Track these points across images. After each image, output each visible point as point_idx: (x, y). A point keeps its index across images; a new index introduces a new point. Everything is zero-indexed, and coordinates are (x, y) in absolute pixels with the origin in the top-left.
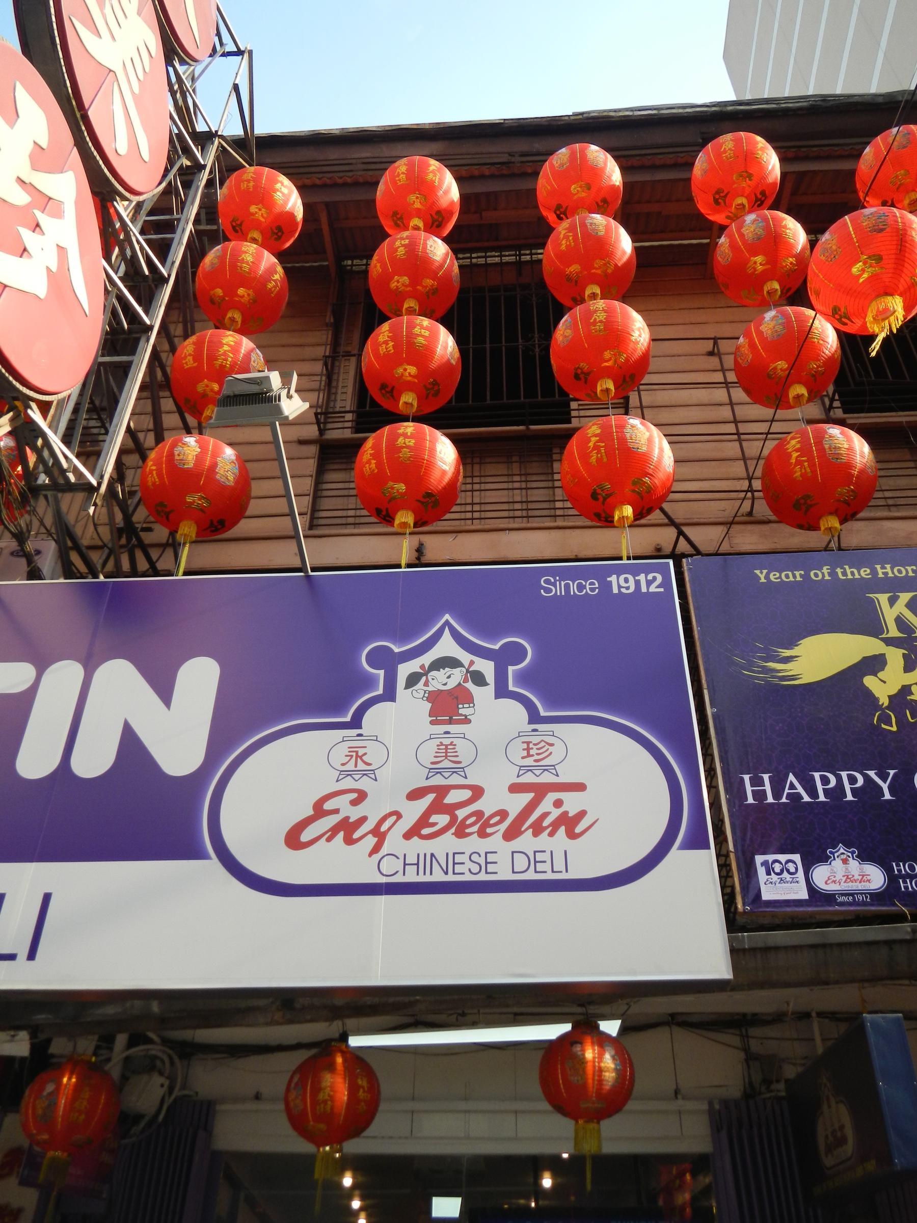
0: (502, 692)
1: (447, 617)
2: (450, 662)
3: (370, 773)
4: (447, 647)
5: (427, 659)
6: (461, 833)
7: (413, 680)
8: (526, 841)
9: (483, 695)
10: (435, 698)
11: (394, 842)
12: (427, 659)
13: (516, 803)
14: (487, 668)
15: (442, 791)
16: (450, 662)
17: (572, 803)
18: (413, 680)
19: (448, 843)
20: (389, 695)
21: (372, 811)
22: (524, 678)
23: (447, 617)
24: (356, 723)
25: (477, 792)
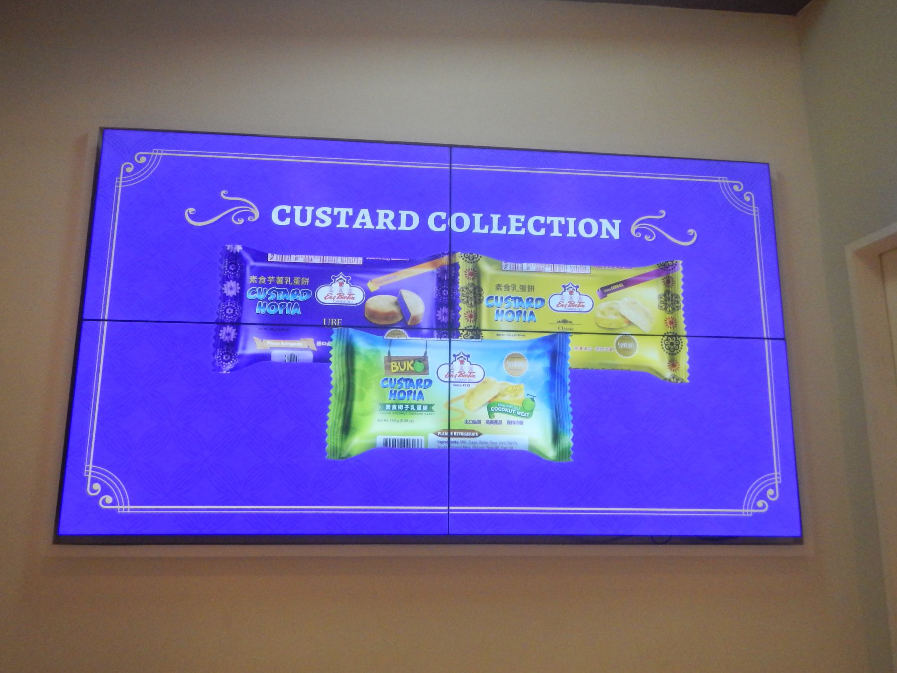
0: (347, 283)
1: (341, 273)
2: (341, 279)
3: (333, 291)
4: (341, 277)
5: (339, 278)
6: (342, 298)
7: (337, 281)
8: (349, 300)
9: (345, 283)
10: (340, 283)
11: (336, 299)
12: (339, 278)
13: (348, 296)
14: (345, 279)
15: (340, 294)
16: (341, 279)
17: (353, 296)
18: (337, 281)
19: (340, 300)
20: (335, 282)
21: (333, 296)
22: (349, 281)
23: (341, 273)
24: (331, 286)
25: (344, 294)
